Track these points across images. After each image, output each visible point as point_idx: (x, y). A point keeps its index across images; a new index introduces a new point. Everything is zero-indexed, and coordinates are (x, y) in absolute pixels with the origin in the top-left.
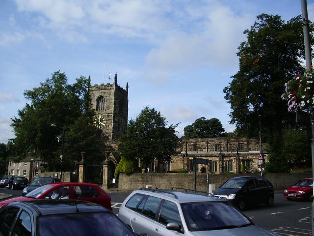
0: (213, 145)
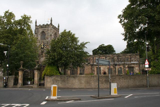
0: (110, 59)
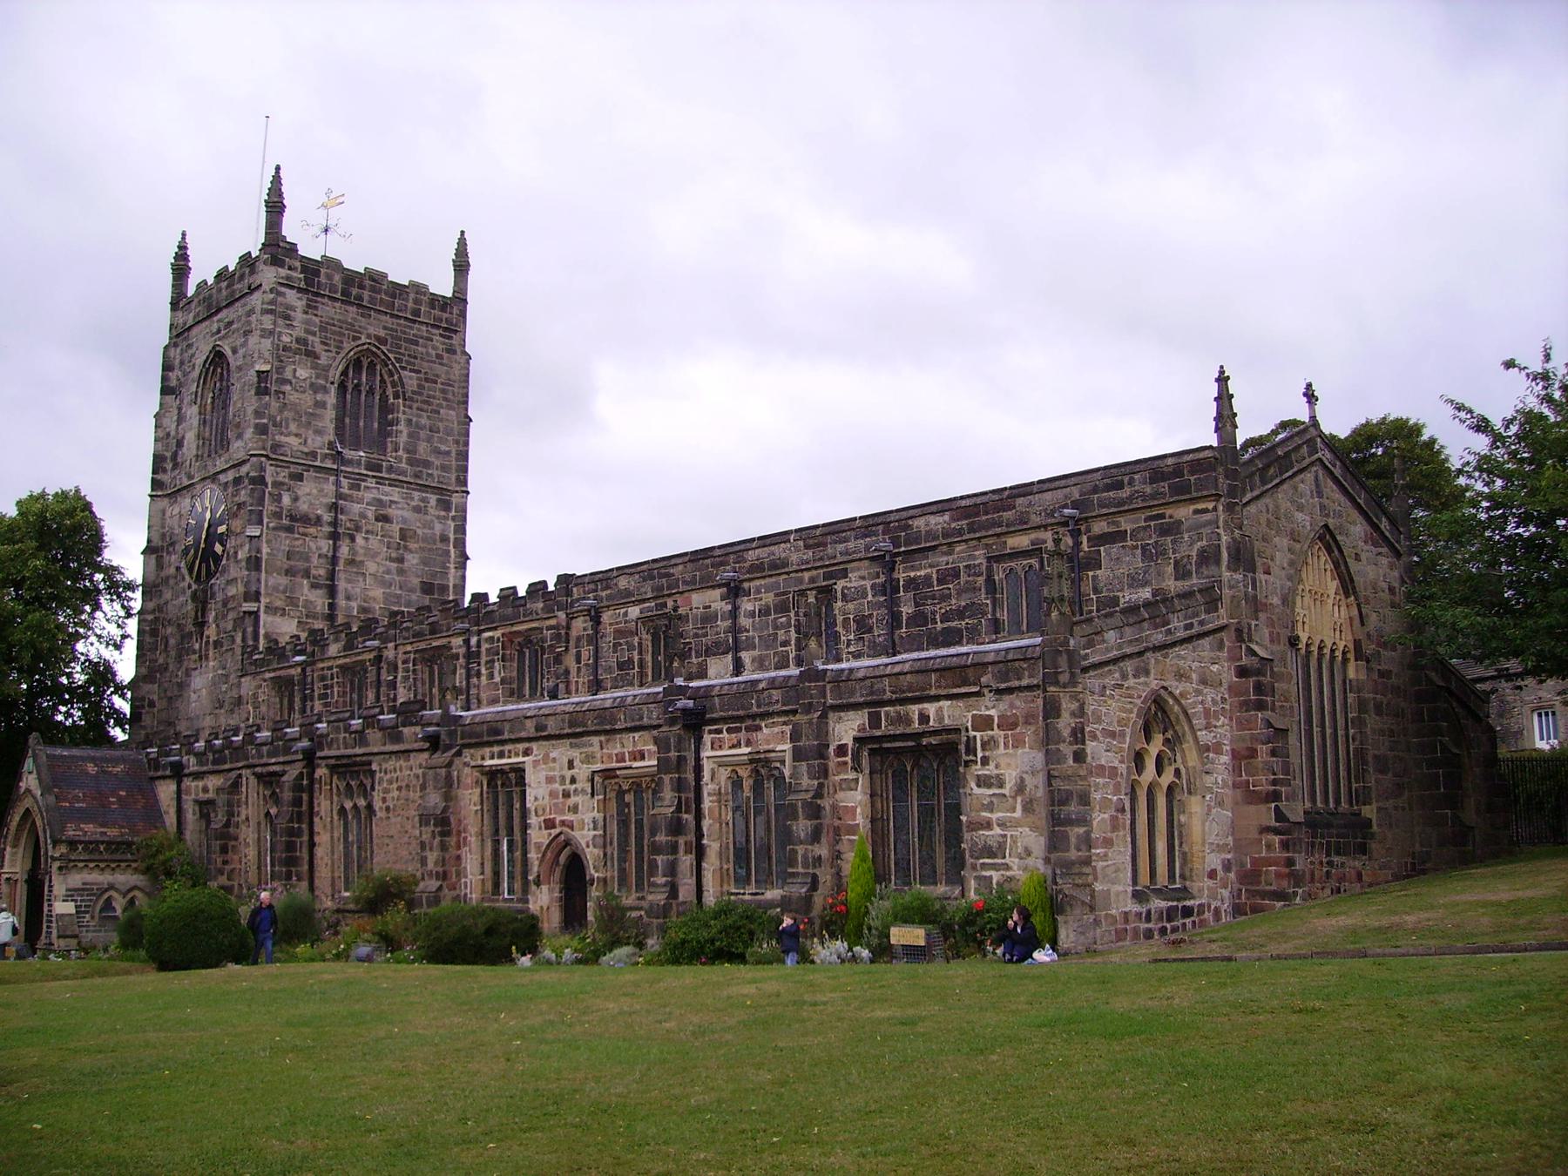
0: (782, 608)
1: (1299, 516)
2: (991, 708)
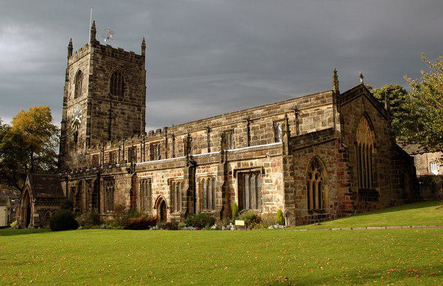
1: (358, 109)
2: (269, 161)
